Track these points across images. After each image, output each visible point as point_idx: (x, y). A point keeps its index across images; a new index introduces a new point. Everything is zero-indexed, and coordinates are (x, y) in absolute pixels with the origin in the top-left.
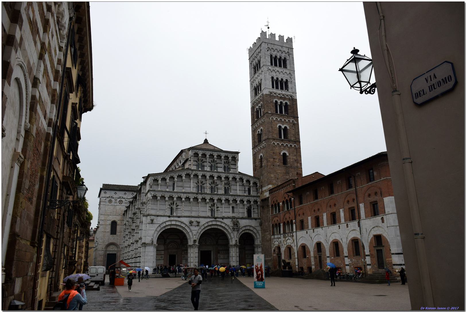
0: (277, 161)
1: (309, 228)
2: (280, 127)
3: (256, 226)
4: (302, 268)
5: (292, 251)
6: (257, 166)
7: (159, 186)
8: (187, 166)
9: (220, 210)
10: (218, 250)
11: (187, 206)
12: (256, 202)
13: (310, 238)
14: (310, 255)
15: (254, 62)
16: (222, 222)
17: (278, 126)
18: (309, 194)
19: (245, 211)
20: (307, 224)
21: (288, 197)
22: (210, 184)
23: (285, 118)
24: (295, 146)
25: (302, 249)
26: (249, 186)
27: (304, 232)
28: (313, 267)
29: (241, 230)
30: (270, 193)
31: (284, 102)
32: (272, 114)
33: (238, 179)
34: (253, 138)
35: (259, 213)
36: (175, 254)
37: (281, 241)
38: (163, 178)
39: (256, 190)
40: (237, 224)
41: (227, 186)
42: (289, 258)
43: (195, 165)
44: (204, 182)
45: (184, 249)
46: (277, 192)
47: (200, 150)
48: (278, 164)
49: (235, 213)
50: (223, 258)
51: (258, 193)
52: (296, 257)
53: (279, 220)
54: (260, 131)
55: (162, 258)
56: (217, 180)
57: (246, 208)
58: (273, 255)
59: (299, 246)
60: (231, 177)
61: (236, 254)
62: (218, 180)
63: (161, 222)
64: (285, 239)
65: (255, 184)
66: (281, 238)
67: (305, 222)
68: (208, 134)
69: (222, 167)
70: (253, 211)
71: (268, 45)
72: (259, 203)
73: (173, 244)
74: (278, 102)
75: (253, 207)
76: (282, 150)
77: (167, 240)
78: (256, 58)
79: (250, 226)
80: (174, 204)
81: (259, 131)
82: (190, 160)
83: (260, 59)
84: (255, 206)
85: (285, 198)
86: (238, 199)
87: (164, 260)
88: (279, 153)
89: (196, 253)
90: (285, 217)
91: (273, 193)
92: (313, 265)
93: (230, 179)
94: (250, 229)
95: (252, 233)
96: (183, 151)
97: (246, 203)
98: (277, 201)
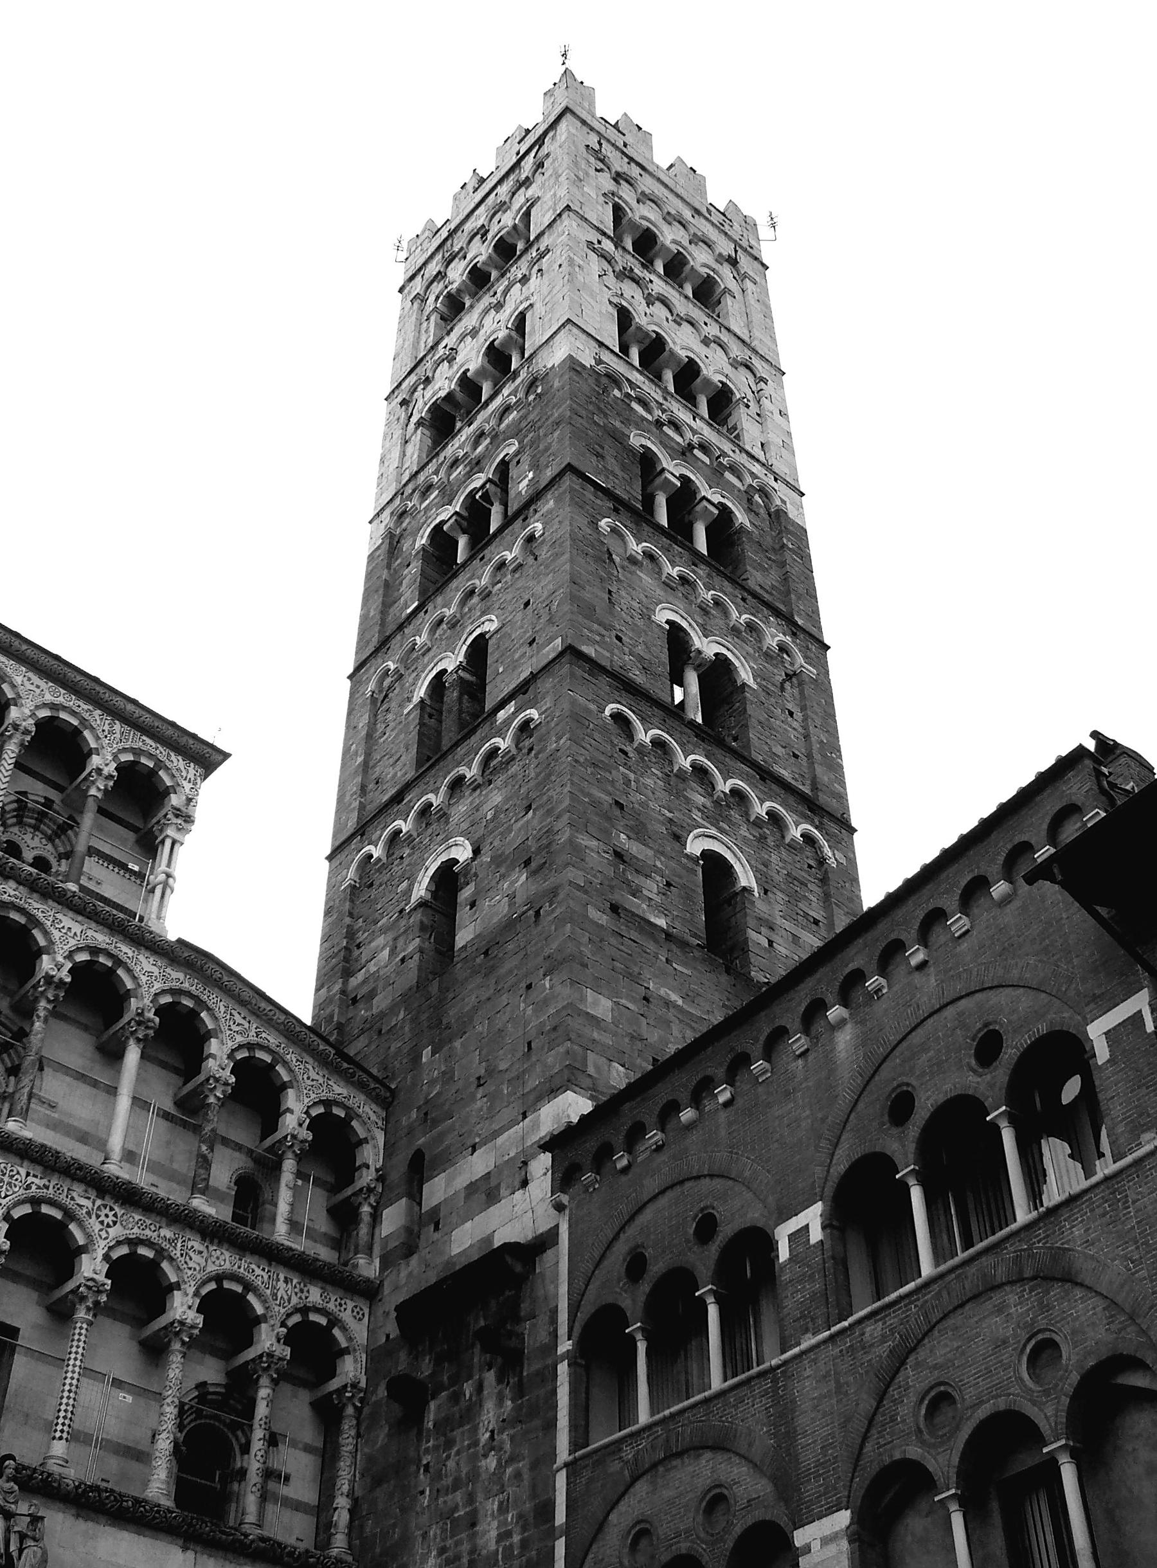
0: (651, 887)
6: (372, 995)
30: (564, 1179)
34: (360, 759)
35: (342, 1502)
48: (661, 922)
72: (351, 1369)
76: (697, 816)
98: (707, 1227)
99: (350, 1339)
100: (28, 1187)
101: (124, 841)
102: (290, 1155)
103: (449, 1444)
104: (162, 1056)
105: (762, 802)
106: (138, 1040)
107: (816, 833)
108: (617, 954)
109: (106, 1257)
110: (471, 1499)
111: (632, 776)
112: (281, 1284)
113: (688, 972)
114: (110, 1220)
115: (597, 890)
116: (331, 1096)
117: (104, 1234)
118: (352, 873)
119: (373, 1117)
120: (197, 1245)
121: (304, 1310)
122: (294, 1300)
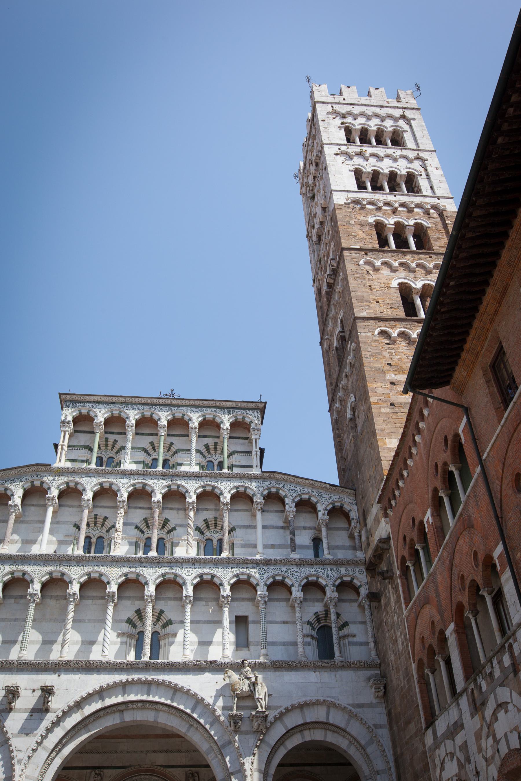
3: (363, 700)
11: (16, 620)
16: (176, 690)
29: (279, 731)
37: (464, 747)
39: (347, 542)
47: (99, 402)
49: (251, 647)
64: (483, 718)
66: (462, 726)
71: (332, 107)
72: (363, 591)
74: (386, 222)
79: (330, 705)
90: (455, 571)
94: (331, 721)
95: (342, 743)
97: (300, 594)
99: (360, 582)
100: (233, 572)
101: (244, 444)
102: (322, 526)
104: (275, 509)
106: (259, 510)
108: (396, 421)
109: (266, 585)
111: (392, 351)
112: (330, 572)
114: (263, 571)
115: (383, 401)
116: (333, 500)
117: (262, 578)
118: (335, 415)
119: (351, 501)
120: (296, 570)
121: (341, 578)
122: (336, 575)
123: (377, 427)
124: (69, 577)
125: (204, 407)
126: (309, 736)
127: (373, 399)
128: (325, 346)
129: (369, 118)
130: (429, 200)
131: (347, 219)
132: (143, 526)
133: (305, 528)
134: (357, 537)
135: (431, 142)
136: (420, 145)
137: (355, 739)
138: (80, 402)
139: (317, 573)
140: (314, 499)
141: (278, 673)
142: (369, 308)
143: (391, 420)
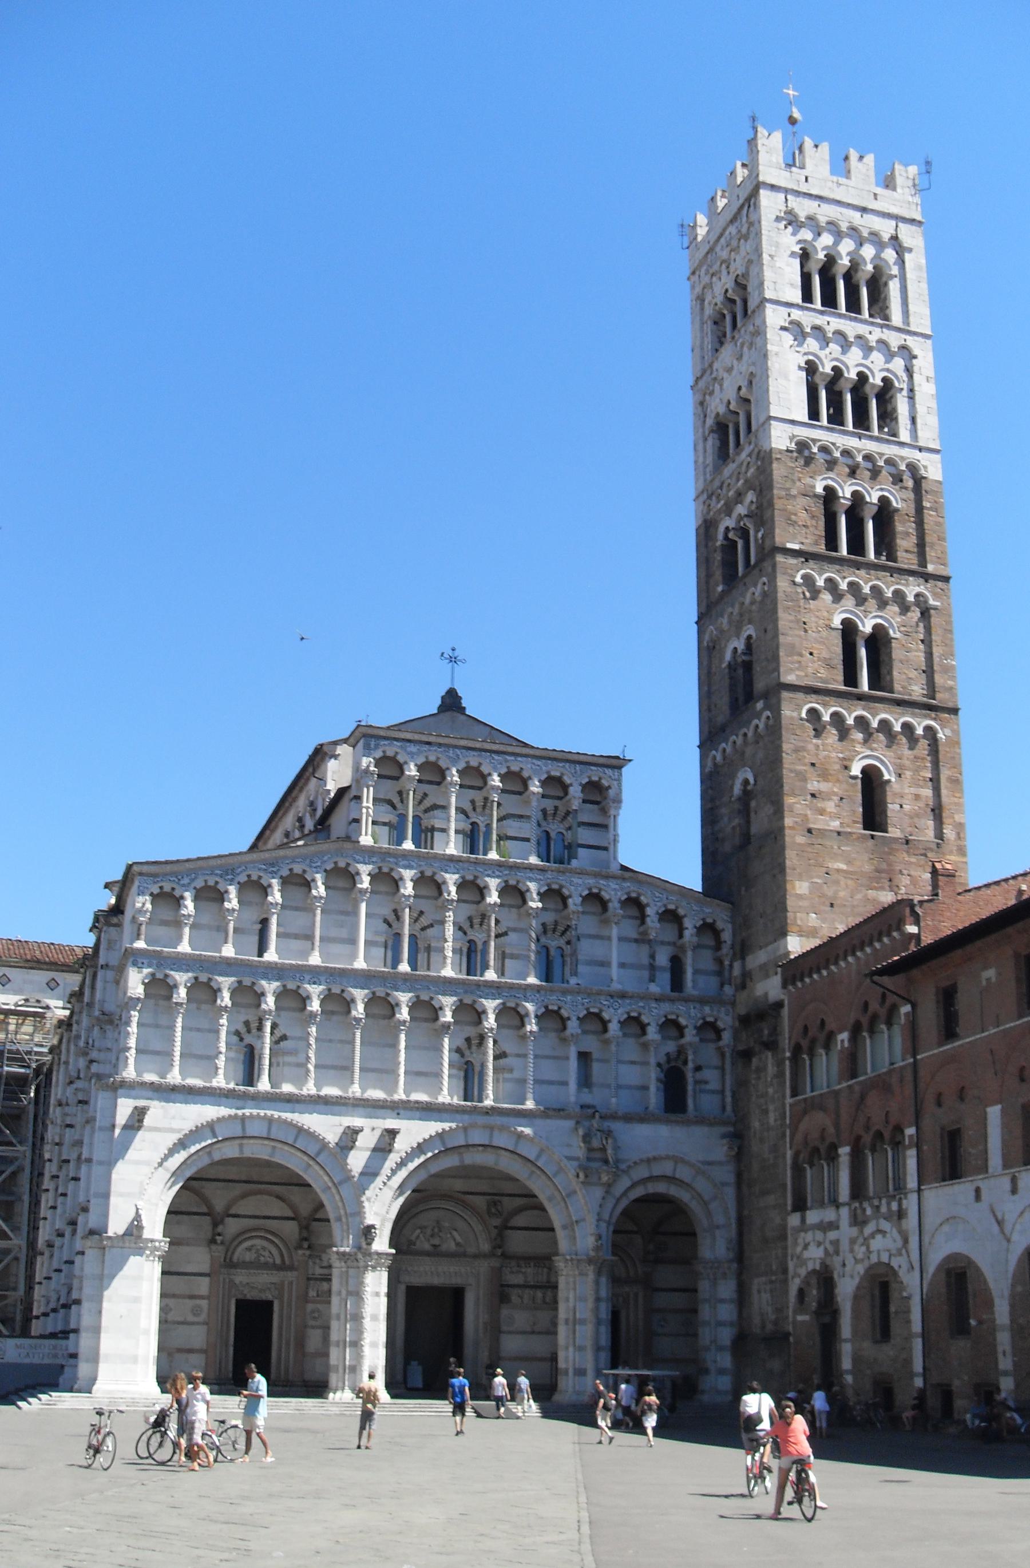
0: (830, 806)
1: (990, 1170)
2: (849, 630)
4: (947, 1395)
5: (894, 1295)
7: (187, 930)
8: (338, 823)
9: (511, 1071)
10: (502, 1286)
11: (330, 1041)
12: (709, 1029)
13: (996, 1228)
14: (994, 1320)
15: (718, 290)
17: (837, 622)
18: (994, 980)
19: (652, 1077)
20: (981, 1147)
21: (884, 996)
22: (460, 929)
23: (878, 579)
24: (928, 729)
25: (948, 1285)
26: (674, 944)
27: (961, 1190)
28: (1007, 1384)
29: (625, 1183)
30: (784, 985)
31: (873, 497)
32: (806, 556)
33: (614, 906)
34: (706, 688)
36: (268, 1296)
37: (836, 1243)
38: (206, 888)
39: (711, 966)
40: (603, 1149)
41: (554, 943)
42: (878, 1336)
43: (385, 824)
44: (424, 921)
45: (318, 1271)
46: (825, 973)
48: (835, 824)
49: (595, 1089)
50: (529, 1329)
51: (722, 985)
52: (917, 1326)
53: (831, 1130)
54: (740, 645)
55: (194, 1315)
56: (501, 905)
57: (659, 1065)
58: (795, 1313)
59: (931, 1269)
60: (576, 889)
61: (596, 1309)
62: (506, 909)
63: (188, 1126)
64: (861, 1232)
65: (708, 928)
66: (838, 1228)
67: (969, 1134)
68: (464, 661)
69: (527, 840)
70: (697, 1082)
72: (727, 1037)
73: (258, 1242)
74: (841, 495)
75: (693, 1061)
76: (858, 748)
77: (230, 1221)
78: (724, 266)
79: (677, 1160)
80: (260, 1028)
81: (735, 649)
82: (358, 798)
83: (747, 268)
84: (709, 1054)
85: (866, 1005)
86: (614, 1015)
87: (207, 1324)
88: (845, 763)
89: (377, 1294)
91: (802, 980)
92: (1006, 1373)
93: (574, 903)
94: (677, 1176)
96: (325, 748)
97: (657, 1037)
98: (823, 1022)
103: (759, 1078)
105: (897, 720)
107: (932, 723)
108: (811, 856)
109: (619, 1022)
110: (766, 1104)
113: (848, 849)
120: (654, 1005)
122: (699, 1015)
123: (788, 863)
124: (396, 998)
125: (550, 759)
126: (652, 1188)
127: (788, 821)
128: (707, 637)
129: (839, 235)
130: (906, 452)
131: (788, 485)
132: (466, 926)
133: (662, 943)
134: (727, 967)
135: (927, 311)
136: (912, 319)
137: (699, 1195)
138: (385, 738)
139: (677, 1011)
140: (681, 912)
141: (628, 1126)
142: (801, 666)
143: (805, 854)
